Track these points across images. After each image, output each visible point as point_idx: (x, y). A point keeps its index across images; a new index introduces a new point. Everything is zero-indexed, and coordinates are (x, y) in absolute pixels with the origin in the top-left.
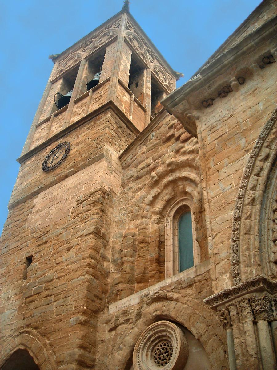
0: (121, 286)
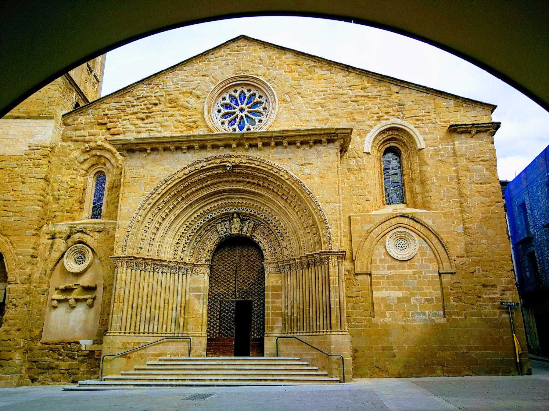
0: (57, 214)
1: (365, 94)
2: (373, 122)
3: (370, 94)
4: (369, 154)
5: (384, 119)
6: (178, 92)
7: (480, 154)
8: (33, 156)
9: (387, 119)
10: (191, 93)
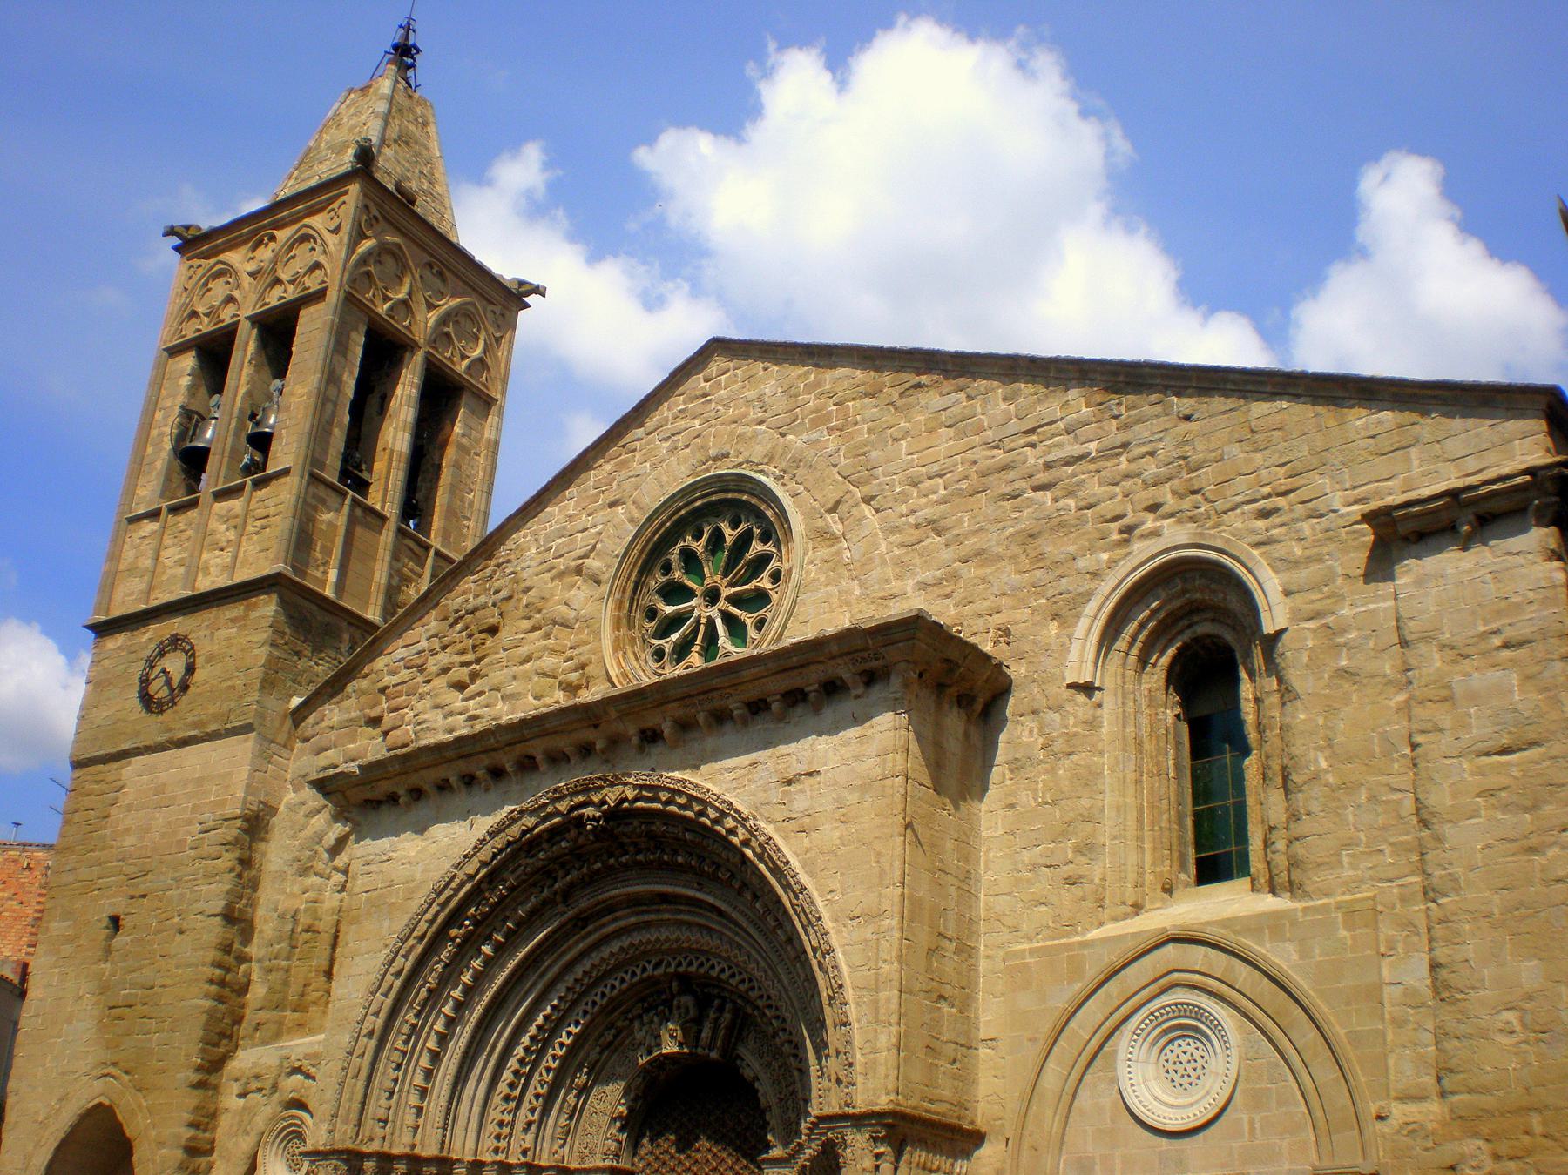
1: (1077, 450)
2: (1105, 556)
3: (1092, 446)
4: (1088, 689)
5: (1143, 537)
6: (547, 576)
7: (1499, 613)
8: (206, 849)
9: (1155, 533)
10: (578, 571)
